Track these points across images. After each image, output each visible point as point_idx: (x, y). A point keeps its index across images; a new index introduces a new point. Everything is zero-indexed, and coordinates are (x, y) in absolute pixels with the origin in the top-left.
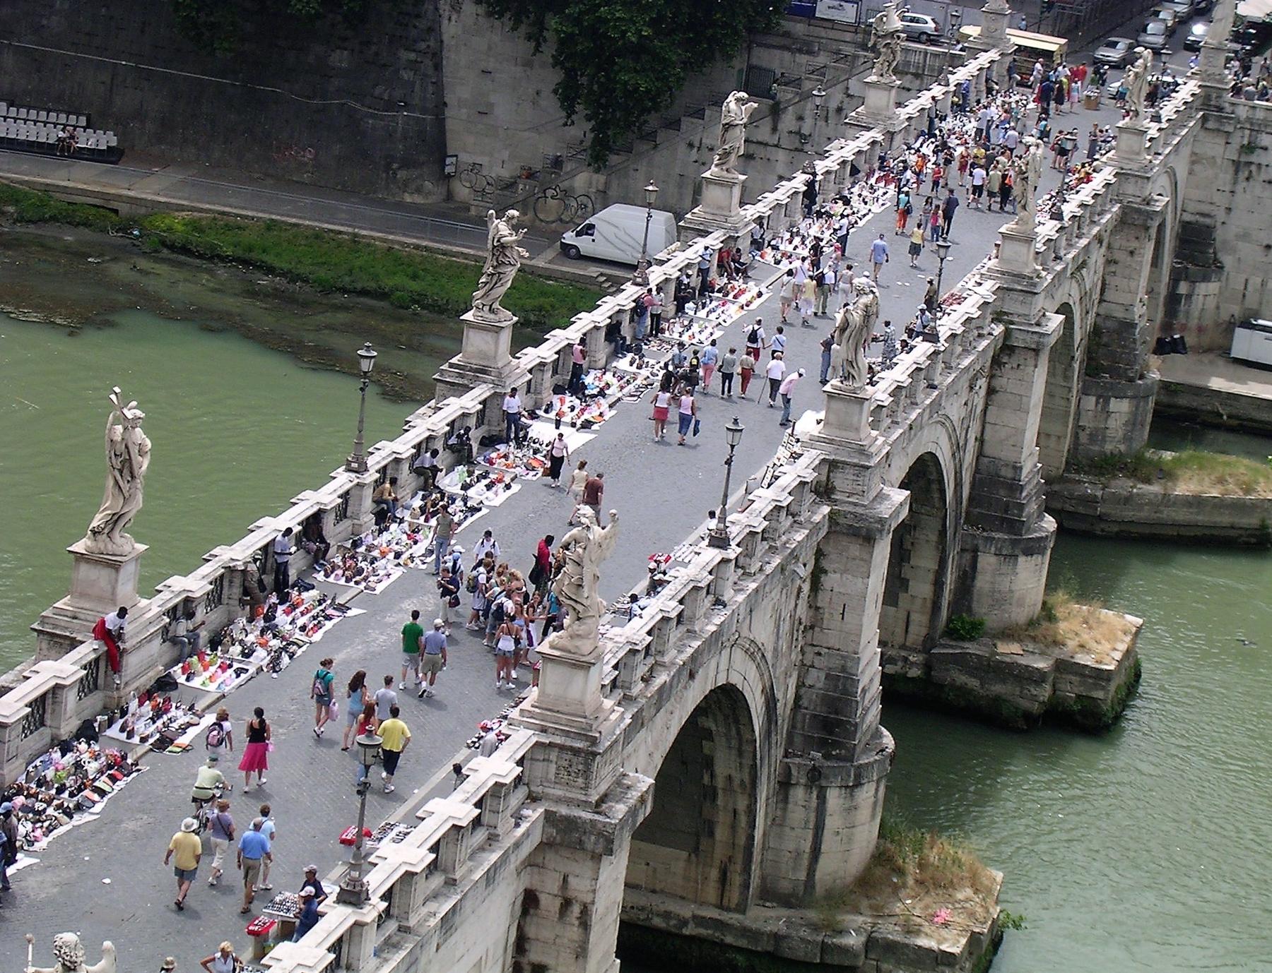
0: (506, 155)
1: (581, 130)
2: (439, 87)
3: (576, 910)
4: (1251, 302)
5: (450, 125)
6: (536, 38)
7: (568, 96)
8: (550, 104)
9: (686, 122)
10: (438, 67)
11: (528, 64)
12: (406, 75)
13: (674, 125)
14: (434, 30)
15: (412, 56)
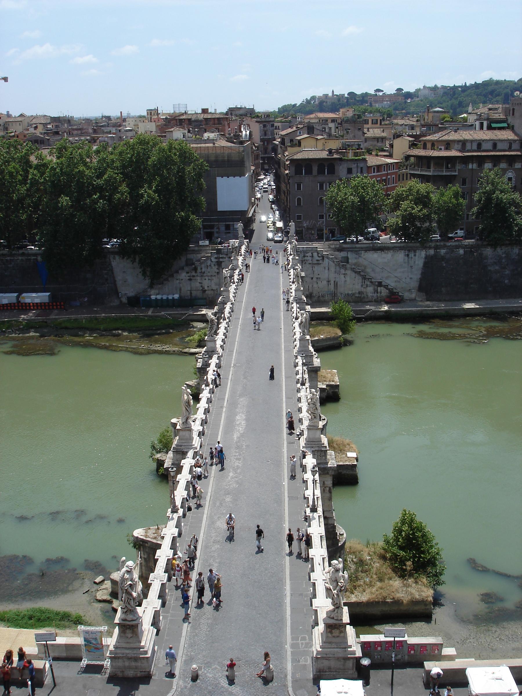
0: (132, 290)
1: (148, 281)
2: (114, 277)
3: (328, 489)
4: (311, 291)
5: (118, 286)
6: (133, 261)
7: (144, 274)
8: (141, 276)
9: (175, 275)
10: (113, 273)
11: (134, 268)
12: (106, 276)
13: (172, 276)
14: (110, 264)
15: (106, 272)
